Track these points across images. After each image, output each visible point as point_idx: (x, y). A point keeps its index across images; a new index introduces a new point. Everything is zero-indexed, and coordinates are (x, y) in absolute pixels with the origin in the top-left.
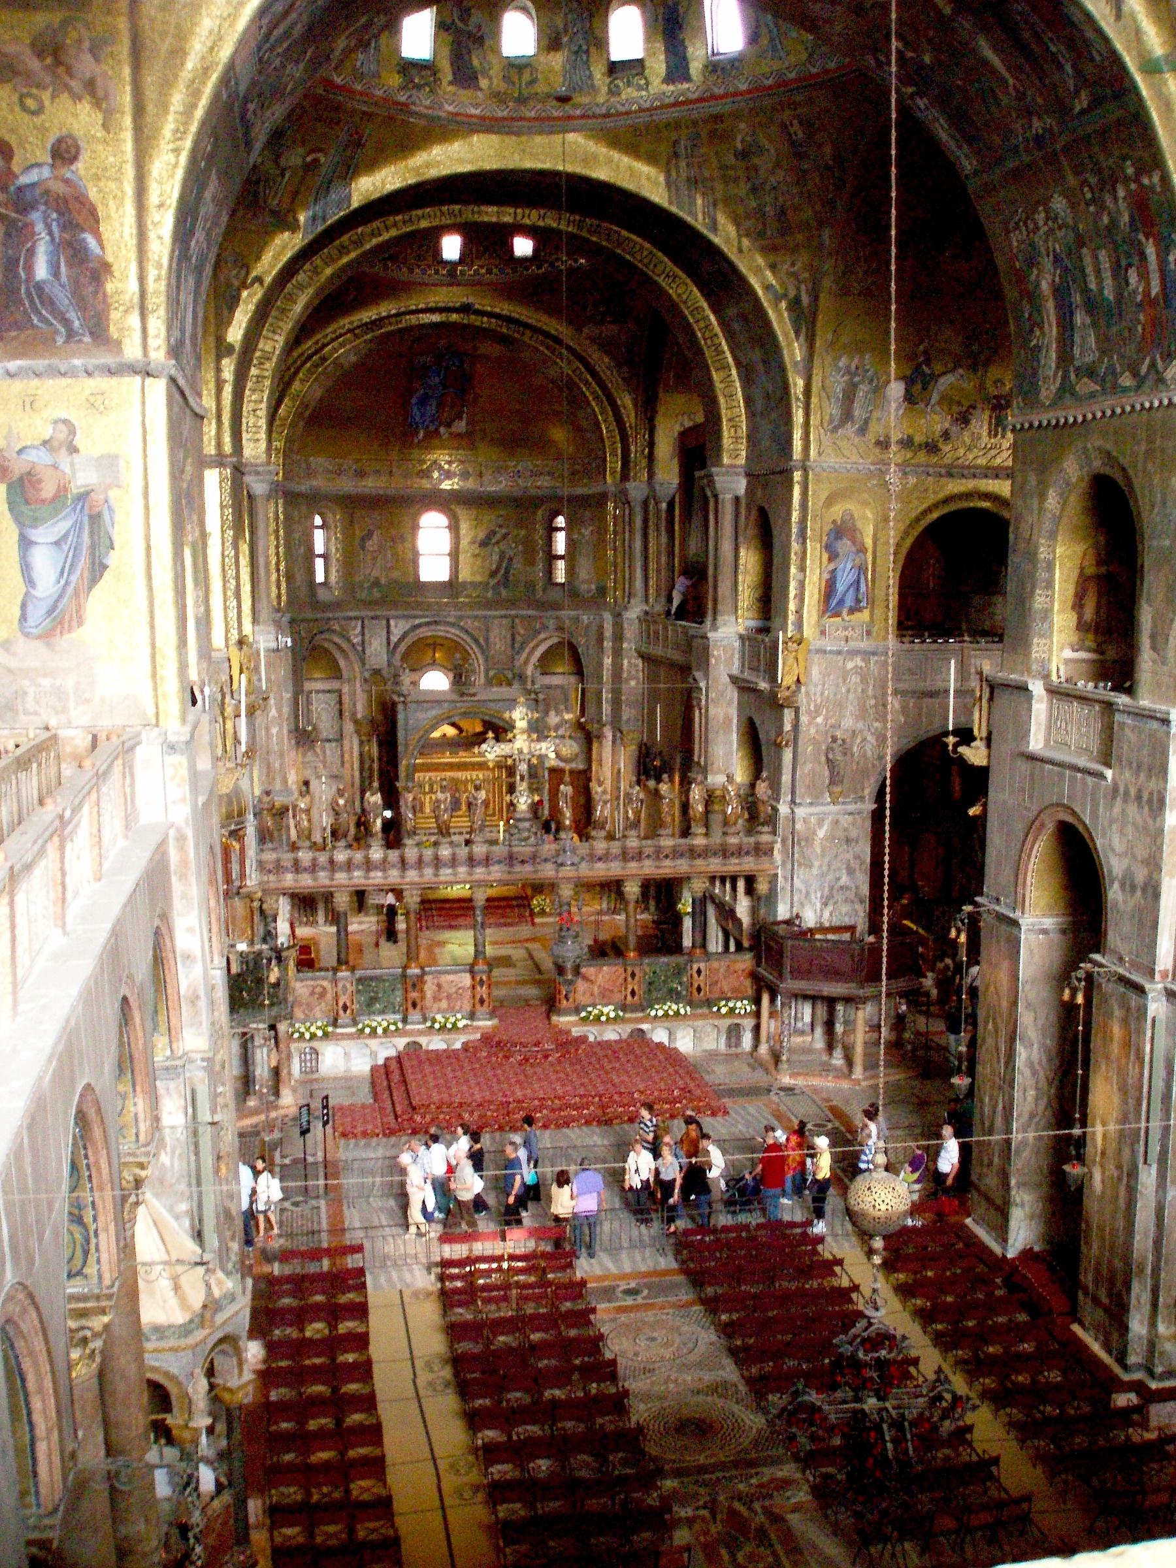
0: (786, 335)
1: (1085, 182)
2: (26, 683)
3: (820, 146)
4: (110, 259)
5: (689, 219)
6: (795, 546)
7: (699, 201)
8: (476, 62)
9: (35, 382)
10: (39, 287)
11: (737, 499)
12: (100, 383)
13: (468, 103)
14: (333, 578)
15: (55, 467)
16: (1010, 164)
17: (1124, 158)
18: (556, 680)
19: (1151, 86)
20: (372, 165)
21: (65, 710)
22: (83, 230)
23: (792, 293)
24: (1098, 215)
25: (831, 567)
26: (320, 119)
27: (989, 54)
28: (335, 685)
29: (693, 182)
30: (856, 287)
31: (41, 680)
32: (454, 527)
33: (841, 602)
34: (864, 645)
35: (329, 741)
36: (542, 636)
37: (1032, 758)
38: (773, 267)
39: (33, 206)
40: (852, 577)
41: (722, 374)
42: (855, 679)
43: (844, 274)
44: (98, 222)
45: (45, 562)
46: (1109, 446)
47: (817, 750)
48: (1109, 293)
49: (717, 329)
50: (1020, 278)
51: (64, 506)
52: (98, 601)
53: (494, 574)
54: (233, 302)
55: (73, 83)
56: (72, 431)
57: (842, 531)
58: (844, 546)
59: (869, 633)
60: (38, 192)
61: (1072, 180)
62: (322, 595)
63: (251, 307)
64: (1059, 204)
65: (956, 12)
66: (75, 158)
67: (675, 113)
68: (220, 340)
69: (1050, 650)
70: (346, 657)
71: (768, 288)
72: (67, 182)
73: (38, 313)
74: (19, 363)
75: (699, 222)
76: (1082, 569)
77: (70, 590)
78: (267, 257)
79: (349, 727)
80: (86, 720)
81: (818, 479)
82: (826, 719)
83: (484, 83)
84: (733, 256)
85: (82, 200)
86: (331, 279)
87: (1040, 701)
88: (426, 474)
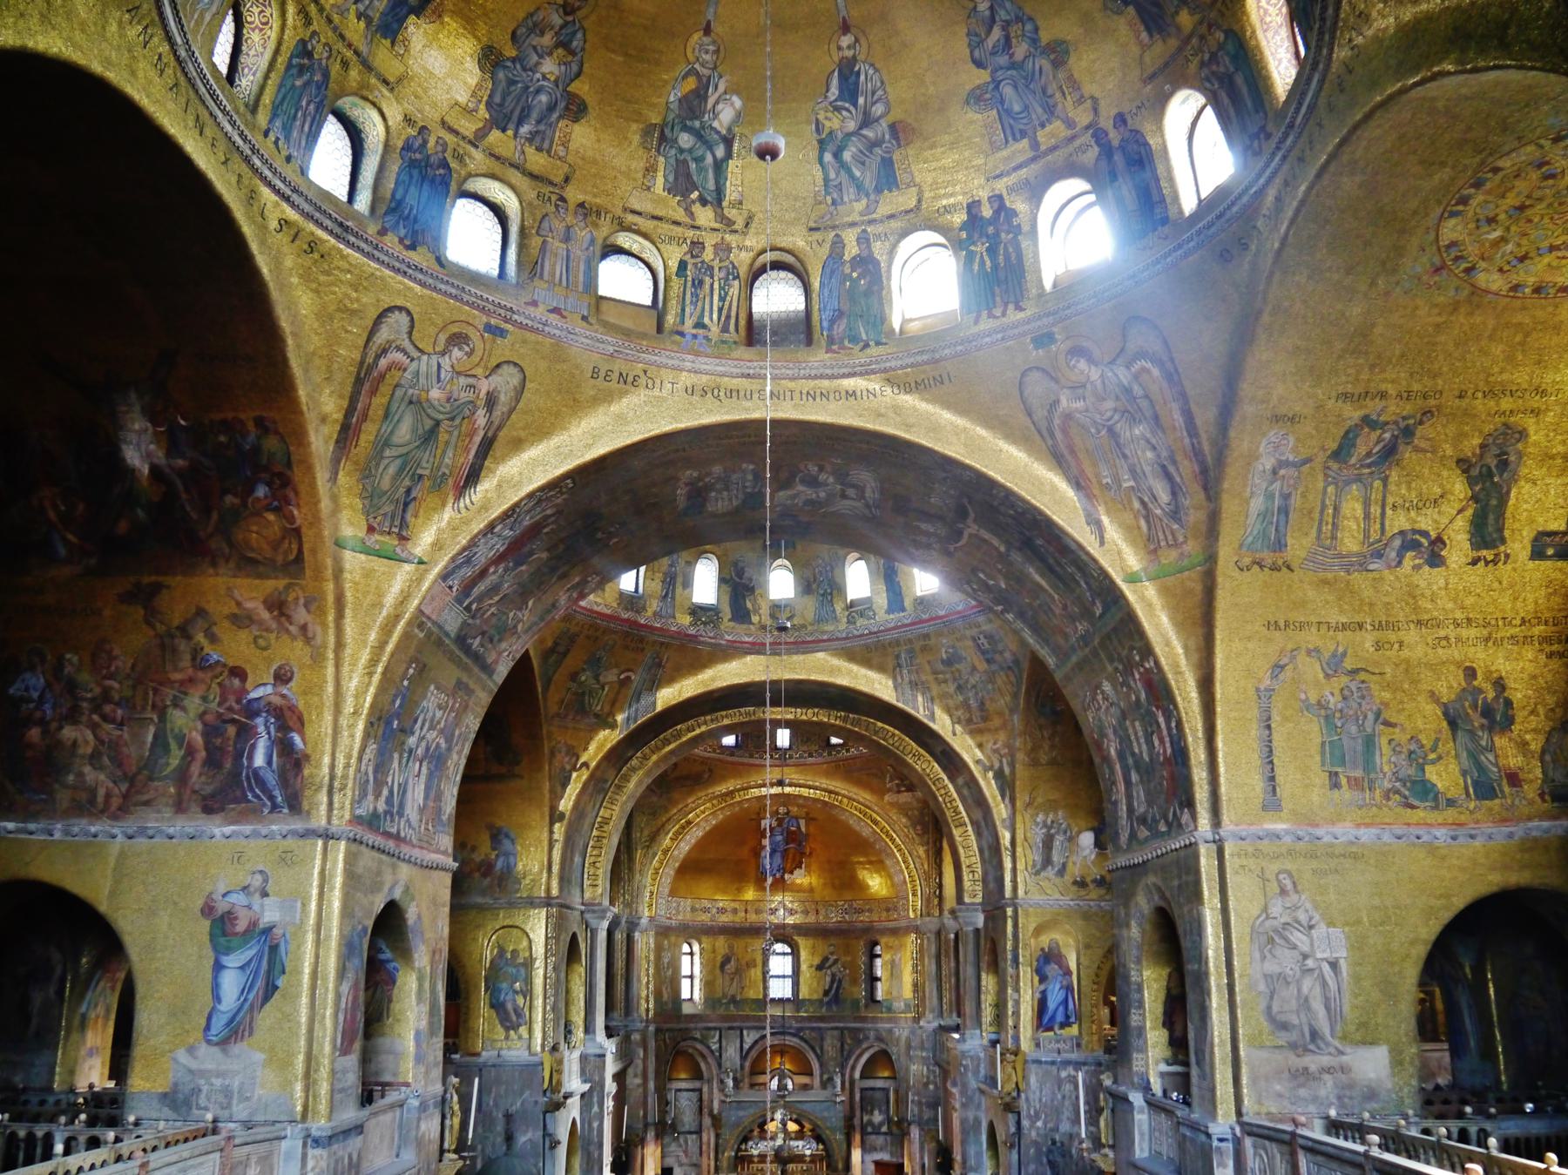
0: (994, 798)
1: (1116, 669)
2: (202, 1082)
3: (1001, 653)
4: (309, 751)
5: (913, 712)
6: (1010, 970)
7: (920, 699)
8: (749, 605)
9: (244, 842)
10: (256, 772)
11: (977, 931)
12: (291, 842)
13: (744, 634)
14: (696, 996)
15: (249, 907)
16: (1074, 659)
17: (1132, 648)
18: (879, 1084)
19: (1135, 592)
20: (671, 680)
21: (229, 1106)
22: (291, 730)
23: (997, 765)
24: (1128, 695)
25: (1042, 987)
26: (626, 647)
27: (1038, 578)
28: (697, 1084)
29: (914, 685)
30: (1044, 758)
31: (214, 1080)
32: (795, 954)
33: (1052, 1018)
34: (1074, 1056)
35: (691, 1133)
36: (864, 1046)
37: (1135, 1166)
38: (980, 746)
39: (257, 714)
40: (1061, 996)
41: (961, 830)
42: (1068, 1087)
43: (1033, 749)
44: (303, 724)
45: (231, 984)
46: (1160, 883)
47: (1038, 1150)
48: (1146, 757)
49: (955, 795)
50: (1099, 746)
51: (252, 938)
52: (266, 1018)
53: (826, 993)
54: (565, 782)
55: (293, 629)
56: (266, 881)
57: (1049, 958)
58: (1052, 969)
59: (1079, 1045)
60: (263, 703)
61: (1110, 668)
62: (687, 1009)
63: (580, 786)
64: (1107, 687)
65: (1008, 550)
66: (290, 679)
67: (895, 635)
68: (553, 808)
69: (1147, 1065)
70: (707, 1063)
71: (978, 762)
72: (283, 696)
73: (252, 791)
74: (233, 827)
75: (920, 714)
76: (1168, 989)
77: (247, 1006)
78: (592, 747)
79: (707, 1121)
80: (243, 1116)
81: (1027, 915)
82: (1045, 1123)
83: (755, 619)
84: (949, 738)
85: (292, 709)
86: (656, 764)
87: (1141, 1112)
88: (774, 911)
